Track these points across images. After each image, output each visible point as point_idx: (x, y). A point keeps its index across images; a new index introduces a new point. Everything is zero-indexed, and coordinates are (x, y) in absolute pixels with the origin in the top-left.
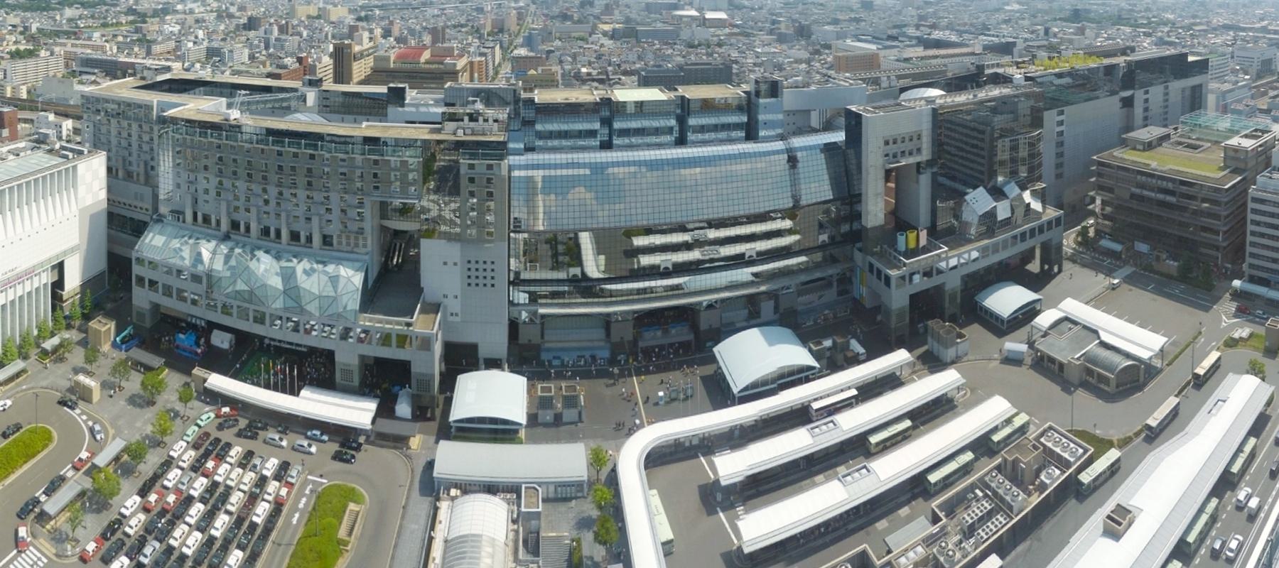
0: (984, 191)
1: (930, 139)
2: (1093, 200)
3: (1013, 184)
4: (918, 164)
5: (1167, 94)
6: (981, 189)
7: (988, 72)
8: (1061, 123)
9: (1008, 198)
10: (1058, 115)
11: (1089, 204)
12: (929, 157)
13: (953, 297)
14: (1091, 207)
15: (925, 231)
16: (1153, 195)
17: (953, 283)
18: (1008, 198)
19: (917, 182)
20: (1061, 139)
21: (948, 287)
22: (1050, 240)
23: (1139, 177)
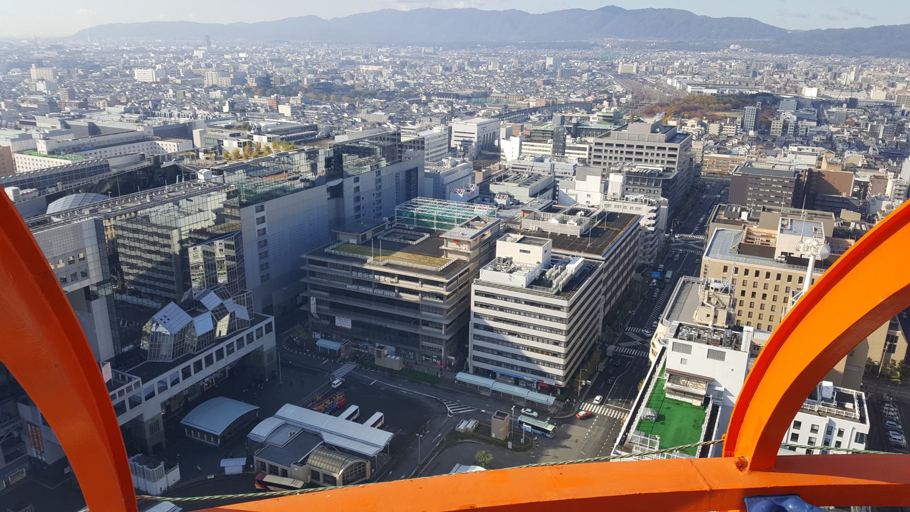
0: (177, 307)
1: (97, 257)
2: (306, 301)
3: (212, 292)
4: (87, 289)
5: (379, 181)
6: (172, 304)
7: (165, 164)
8: (262, 220)
9: (208, 310)
10: (257, 211)
11: (301, 305)
12: (100, 279)
13: (154, 426)
14: (303, 308)
15: (109, 365)
16: (371, 290)
17: (151, 410)
18: (208, 310)
19: (89, 310)
20: (263, 238)
21: (146, 418)
22: (262, 347)
23: (354, 273)
